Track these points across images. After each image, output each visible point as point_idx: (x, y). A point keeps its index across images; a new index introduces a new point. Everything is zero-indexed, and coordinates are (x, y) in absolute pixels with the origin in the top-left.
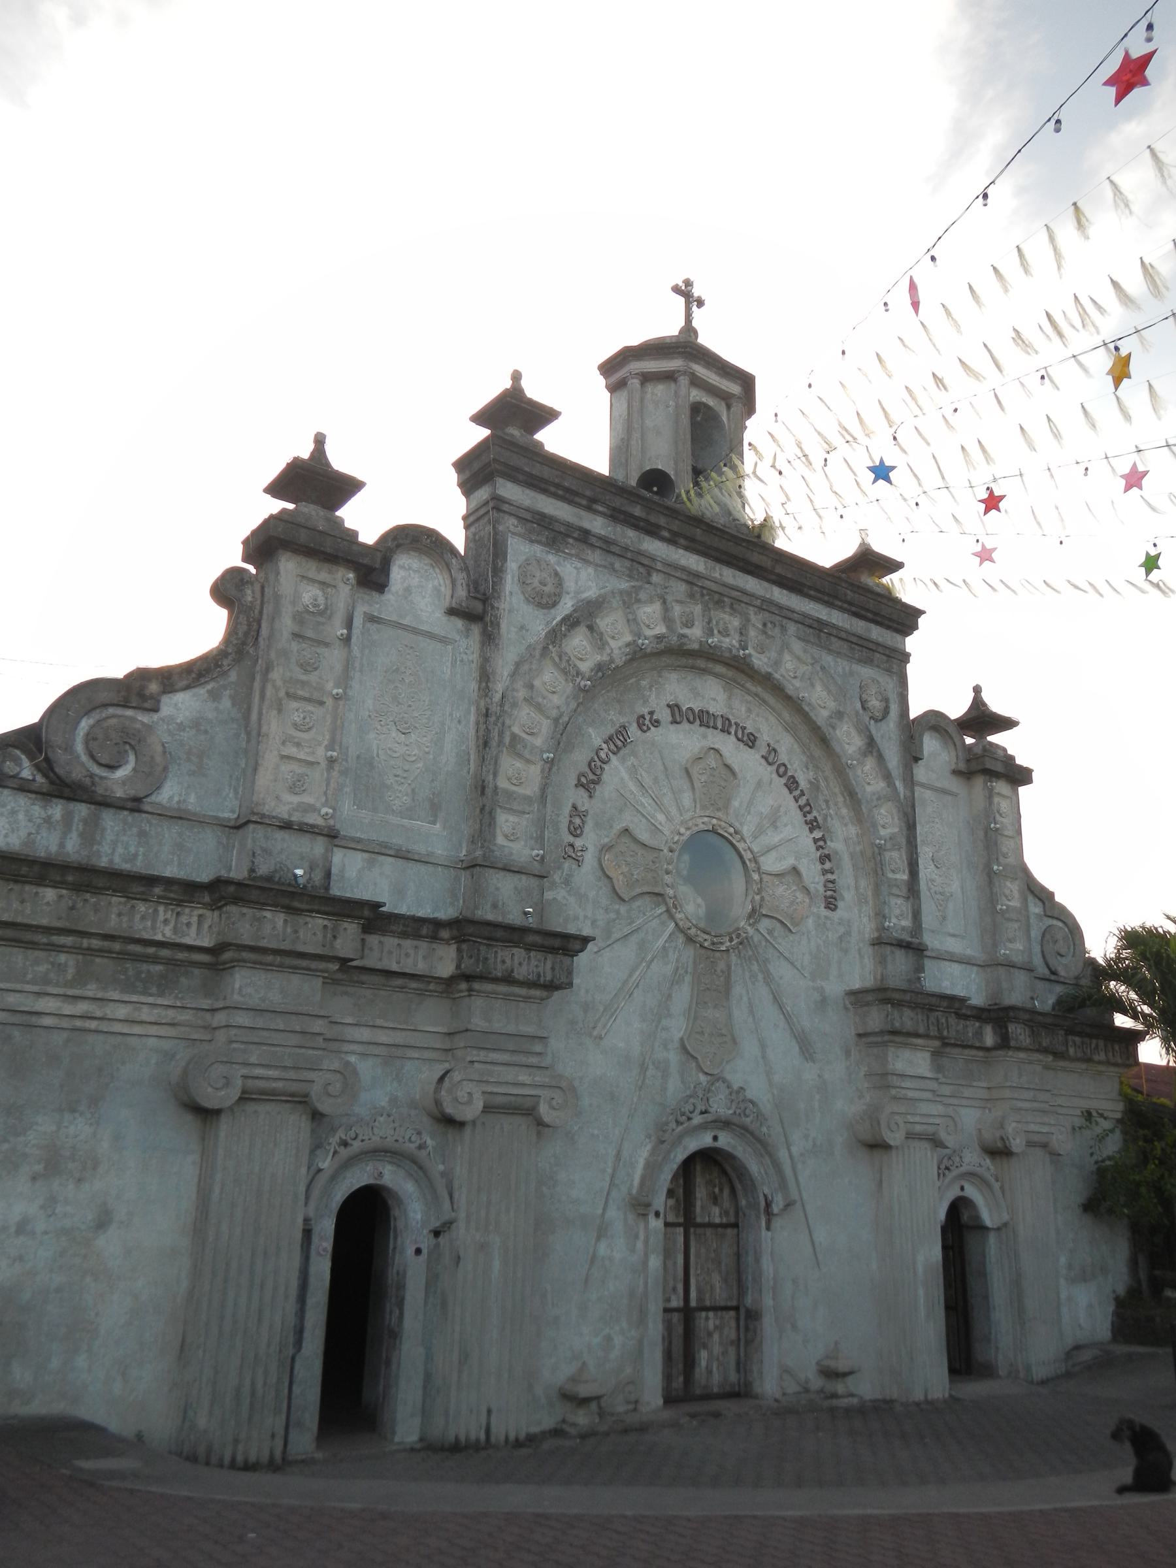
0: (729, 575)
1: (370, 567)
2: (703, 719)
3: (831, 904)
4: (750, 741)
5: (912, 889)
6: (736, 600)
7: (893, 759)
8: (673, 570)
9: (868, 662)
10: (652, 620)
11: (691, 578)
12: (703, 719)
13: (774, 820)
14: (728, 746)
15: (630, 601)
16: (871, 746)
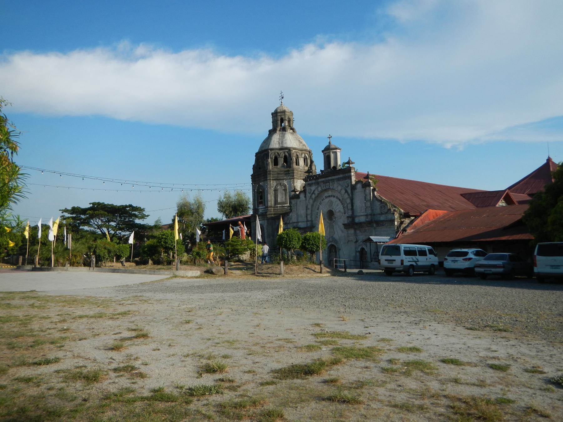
0: (327, 179)
1: (298, 197)
2: (329, 196)
3: (345, 213)
4: (334, 197)
5: (352, 209)
6: (328, 181)
7: (349, 191)
8: (321, 182)
9: (346, 179)
10: (320, 189)
11: (323, 182)
12: (329, 196)
13: (337, 205)
14: (332, 199)
15: (317, 188)
16: (346, 191)
